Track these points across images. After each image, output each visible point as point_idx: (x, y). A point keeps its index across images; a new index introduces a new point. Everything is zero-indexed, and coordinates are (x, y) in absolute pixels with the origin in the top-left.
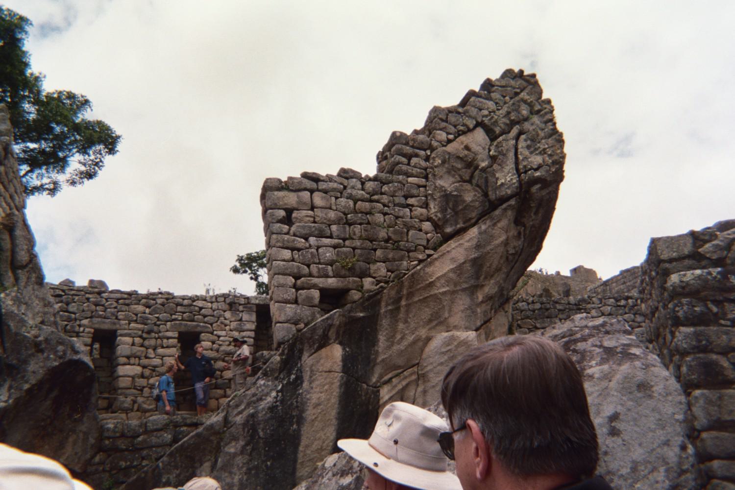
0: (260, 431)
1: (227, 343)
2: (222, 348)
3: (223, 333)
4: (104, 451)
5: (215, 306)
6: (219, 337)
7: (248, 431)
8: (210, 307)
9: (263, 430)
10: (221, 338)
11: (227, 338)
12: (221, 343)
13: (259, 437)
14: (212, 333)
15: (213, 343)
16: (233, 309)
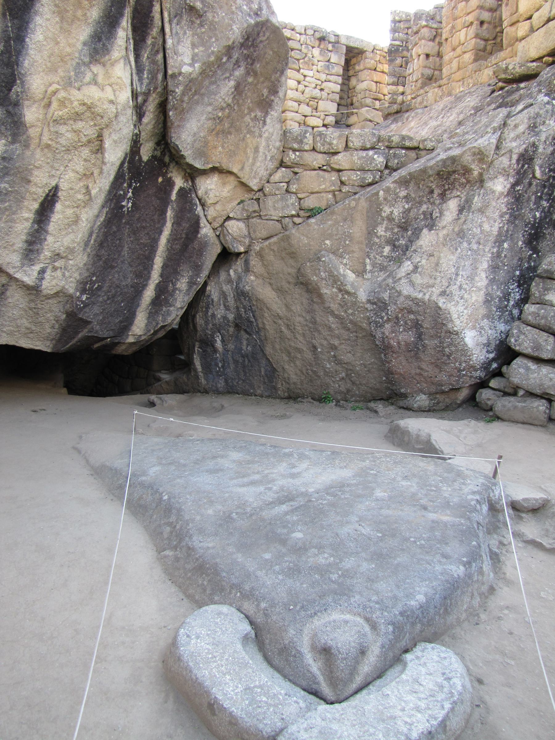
0: (537, 168)
1: (314, 86)
2: (307, 90)
3: (310, 73)
4: (286, 167)
5: (303, 38)
6: (305, 76)
7: (523, 166)
8: (298, 39)
9: (541, 167)
10: (307, 79)
11: (313, 80)
12: (307, 84)
13: (534, 177)
14: (298, 71)
15: (299, 83)
16: (322, 46)
